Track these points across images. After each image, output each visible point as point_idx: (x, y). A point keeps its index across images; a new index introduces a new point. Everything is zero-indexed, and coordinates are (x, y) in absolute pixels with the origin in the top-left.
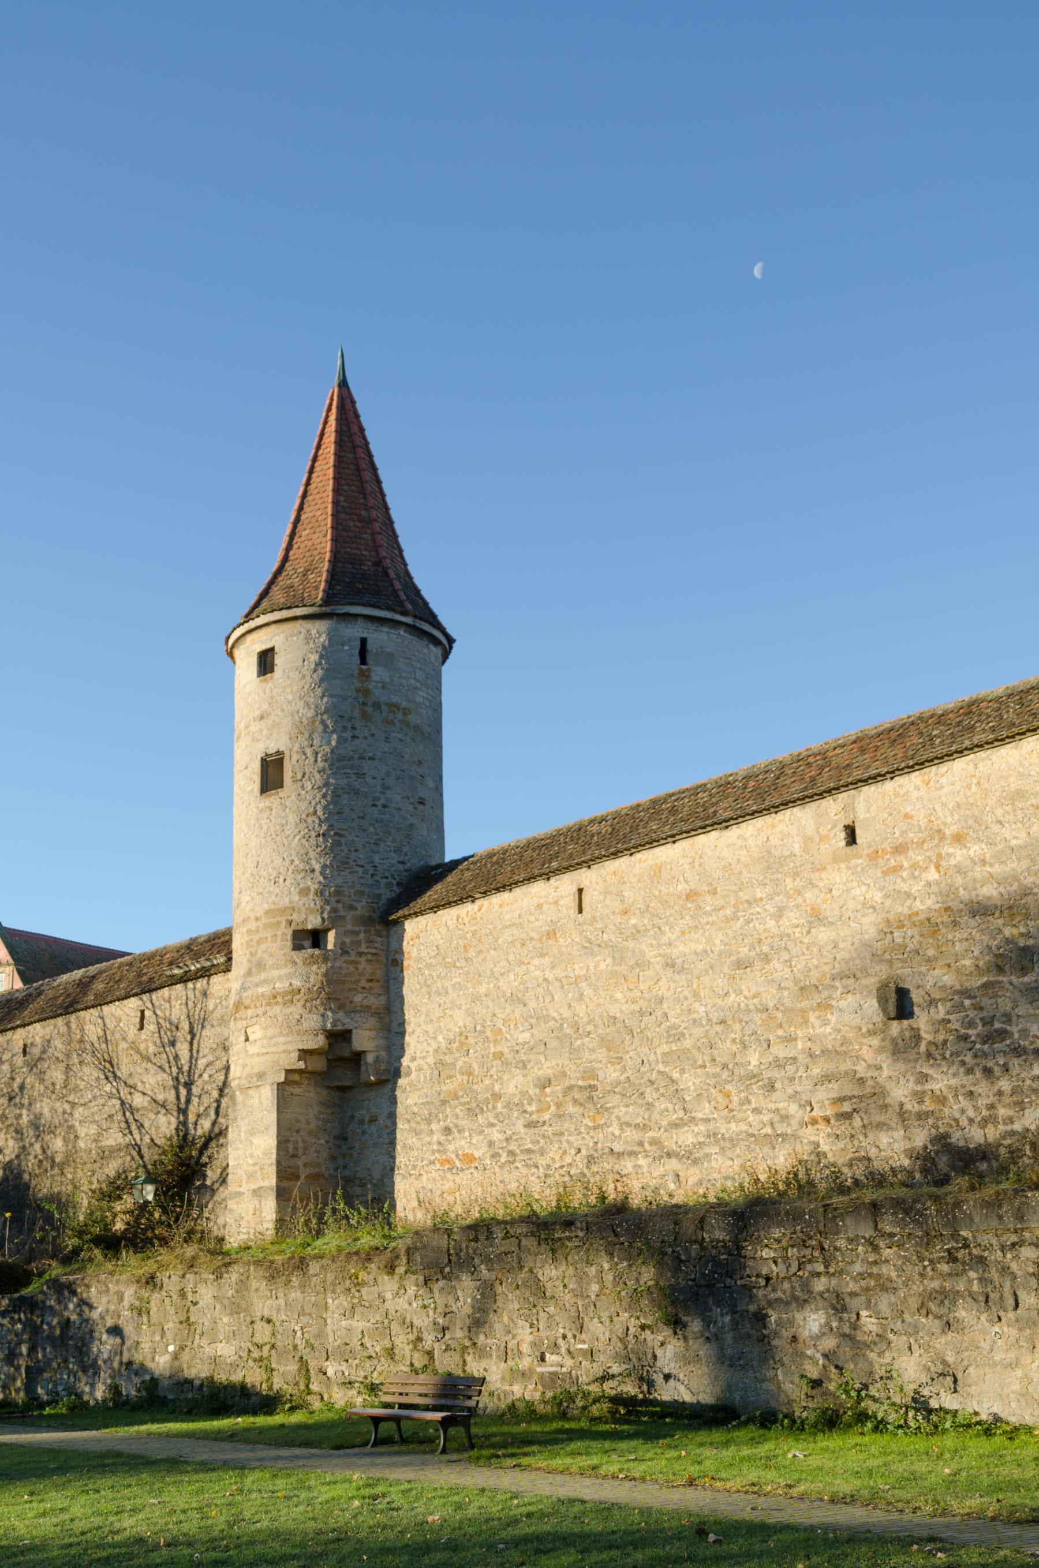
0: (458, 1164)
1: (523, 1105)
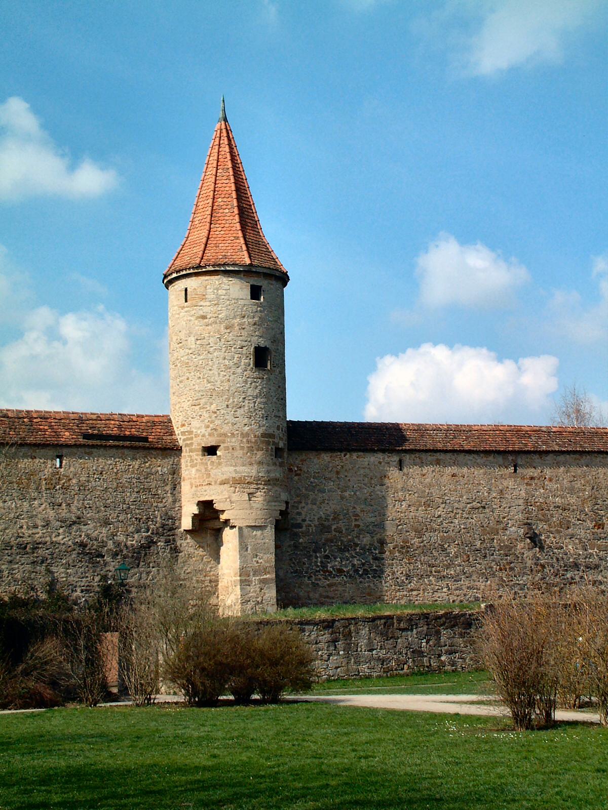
1: (371, 550)
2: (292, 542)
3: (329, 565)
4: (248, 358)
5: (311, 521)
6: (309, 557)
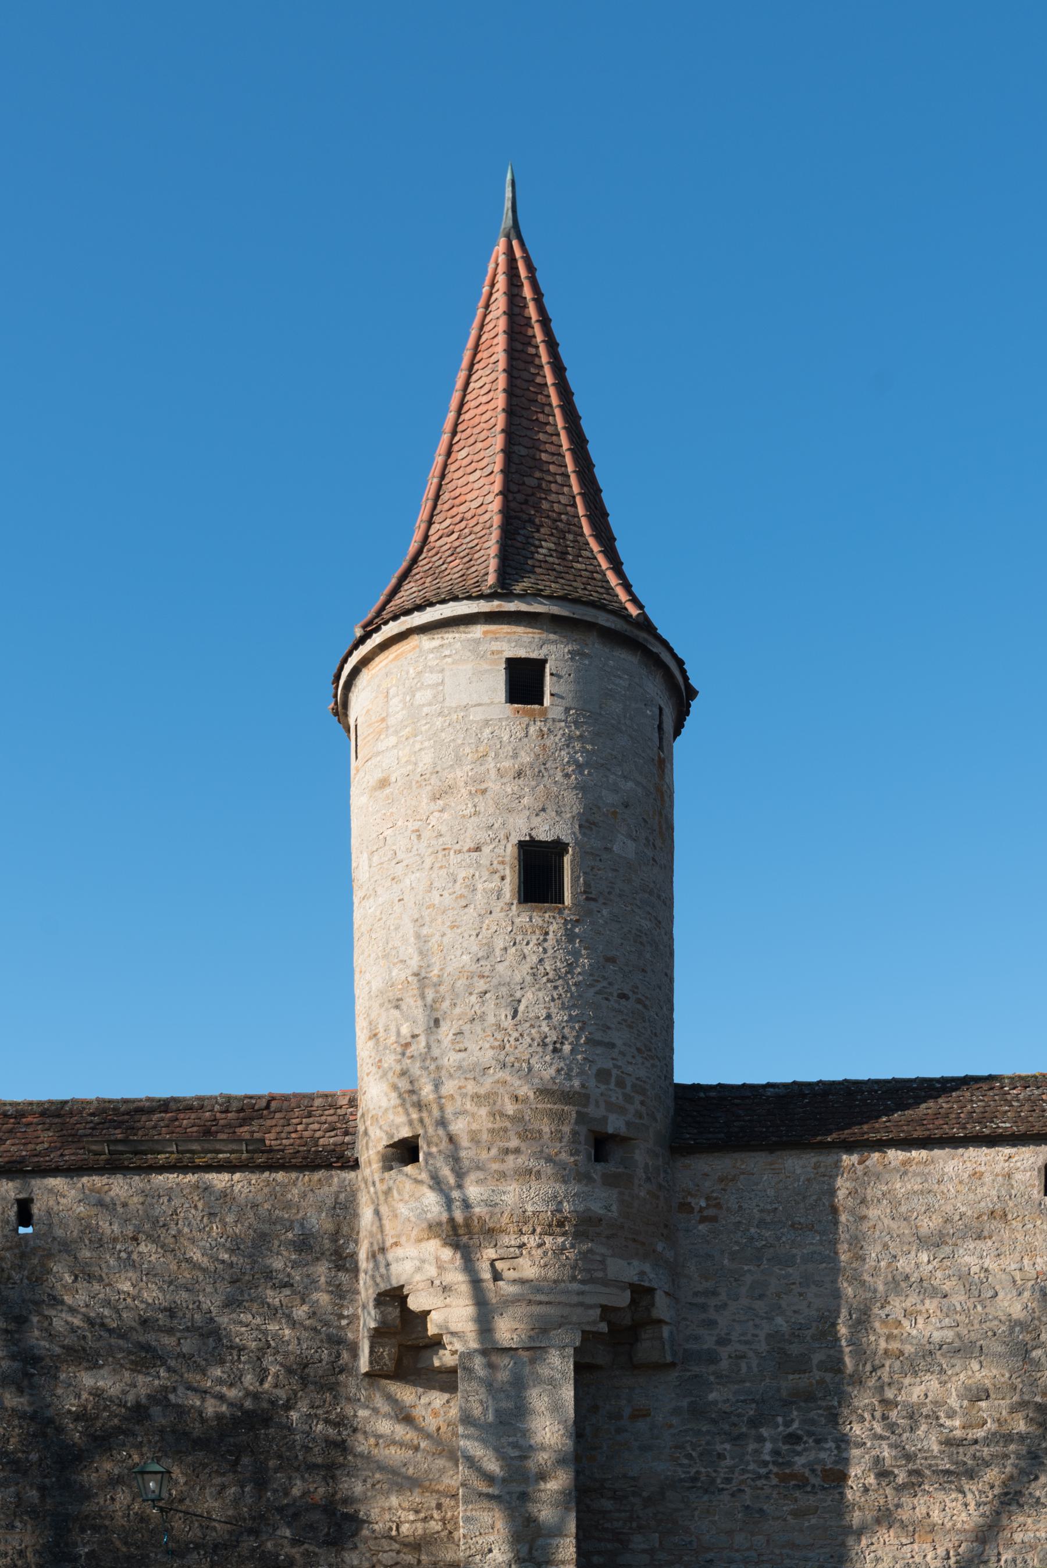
0: (814, 1480)
2: (685, 1403)
3: (800, 1461)
4: (497, 877)
5: (746, 1343)
6: (738, 1439)
